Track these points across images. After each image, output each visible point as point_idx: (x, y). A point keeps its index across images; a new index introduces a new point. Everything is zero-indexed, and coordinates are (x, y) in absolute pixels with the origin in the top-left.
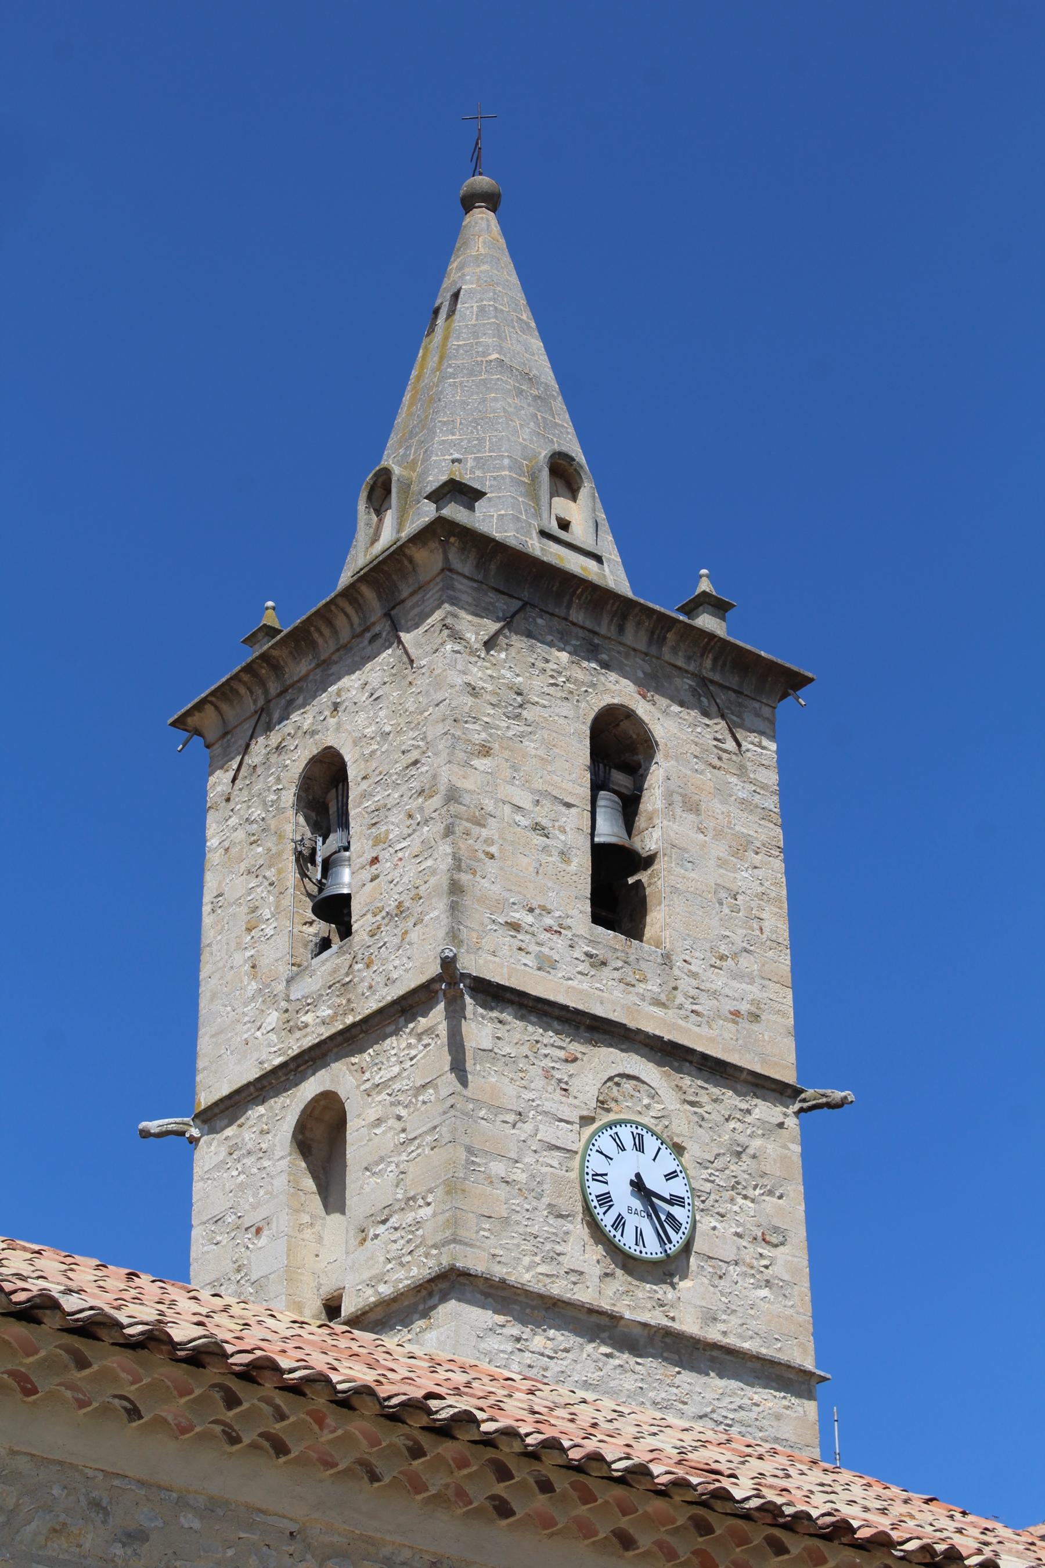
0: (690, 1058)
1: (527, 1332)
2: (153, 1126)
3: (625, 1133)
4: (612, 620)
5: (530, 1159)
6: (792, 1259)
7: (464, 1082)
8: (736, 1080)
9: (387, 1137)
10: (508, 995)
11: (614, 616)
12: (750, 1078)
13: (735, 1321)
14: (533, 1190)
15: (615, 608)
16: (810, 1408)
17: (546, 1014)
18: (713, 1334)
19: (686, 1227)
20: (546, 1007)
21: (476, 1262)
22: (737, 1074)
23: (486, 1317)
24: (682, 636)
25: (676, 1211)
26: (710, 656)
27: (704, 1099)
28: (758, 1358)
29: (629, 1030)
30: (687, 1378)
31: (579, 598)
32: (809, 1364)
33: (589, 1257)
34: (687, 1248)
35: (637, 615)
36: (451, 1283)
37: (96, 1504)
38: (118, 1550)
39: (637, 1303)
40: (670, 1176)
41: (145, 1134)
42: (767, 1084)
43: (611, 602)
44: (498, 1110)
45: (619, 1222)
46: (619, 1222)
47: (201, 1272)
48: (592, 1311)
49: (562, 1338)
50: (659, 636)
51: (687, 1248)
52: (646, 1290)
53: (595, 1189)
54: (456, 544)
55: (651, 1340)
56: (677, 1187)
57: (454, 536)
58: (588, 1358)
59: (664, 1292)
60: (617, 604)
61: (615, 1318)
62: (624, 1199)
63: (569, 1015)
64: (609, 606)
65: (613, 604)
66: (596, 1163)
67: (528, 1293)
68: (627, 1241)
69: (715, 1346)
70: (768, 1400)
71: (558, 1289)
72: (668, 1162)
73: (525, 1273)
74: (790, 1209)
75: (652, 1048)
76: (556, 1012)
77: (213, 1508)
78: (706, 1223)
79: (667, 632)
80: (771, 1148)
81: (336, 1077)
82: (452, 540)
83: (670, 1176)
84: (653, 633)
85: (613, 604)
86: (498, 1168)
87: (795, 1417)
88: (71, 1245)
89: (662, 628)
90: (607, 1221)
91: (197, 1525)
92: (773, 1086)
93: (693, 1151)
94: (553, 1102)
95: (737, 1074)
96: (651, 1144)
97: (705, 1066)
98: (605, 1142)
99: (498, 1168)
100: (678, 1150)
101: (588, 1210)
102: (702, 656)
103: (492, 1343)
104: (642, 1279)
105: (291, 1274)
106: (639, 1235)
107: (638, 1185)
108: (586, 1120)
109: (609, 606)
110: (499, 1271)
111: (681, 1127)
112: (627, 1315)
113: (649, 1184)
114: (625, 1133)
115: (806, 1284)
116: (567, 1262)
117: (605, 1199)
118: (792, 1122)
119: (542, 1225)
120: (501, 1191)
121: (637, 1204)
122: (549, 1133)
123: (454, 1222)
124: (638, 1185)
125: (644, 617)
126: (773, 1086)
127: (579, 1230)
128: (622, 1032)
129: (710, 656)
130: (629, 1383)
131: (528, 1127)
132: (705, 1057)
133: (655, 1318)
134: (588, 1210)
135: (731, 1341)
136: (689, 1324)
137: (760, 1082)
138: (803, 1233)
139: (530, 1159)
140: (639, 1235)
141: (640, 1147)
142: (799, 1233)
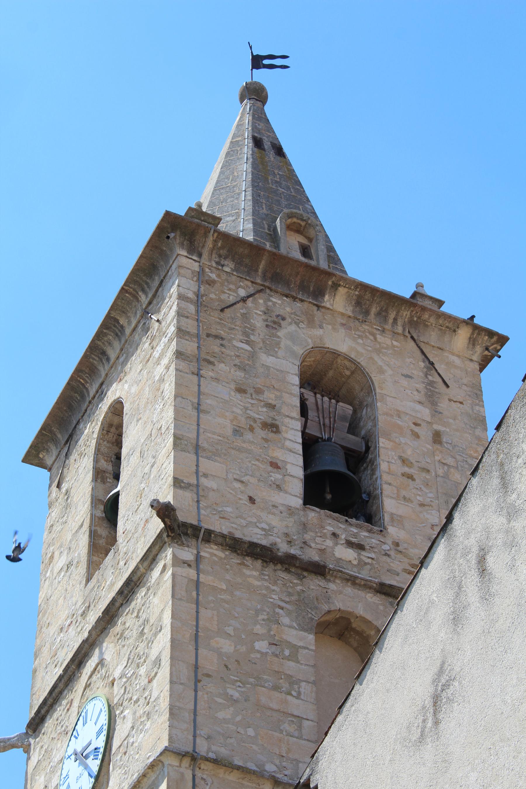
0: (117, 604)
4: (103, 364)
8: (143, 575)
10: (43, 712)
11: (102, 361)
12: (146, 564)
15: (97, 359)
17: (61, 693)
20: (57, 691)
22: (139, 574)
24: (123, 312)
26: (140, 293)
29: (87, 639)
31: (87, 382)
35: (103, 343)
42: (154, 551)
43: (91, 360)
50: (120, 331)
54: (44, 454)
57: (38, 454)
60: (93, 356)
63: (66, 678)
64: (95, 362)
65: (94, 359)
75: (105, 629)
76: (61, 685)
79: (118, 323)
82: (41, 456)
84: (117, 335)
85: (94, 359)
89: (115, 326)
92: (157, 547)
95: (139, 574)
97: (128, 595)
102: (138, 301)
109: (95, 362)
125: (106, 339)
126: (157, 547)
128: (86, 646)
129: (140, 293)
132: (120, 592)
137: (151, 557)
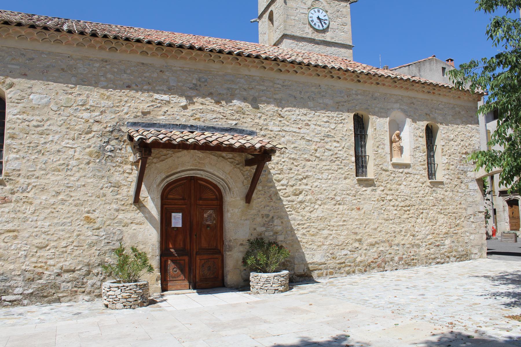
1: (298, 43)
2: (252, 20)
3: (316, 10)
5: (298, 16)
6: (348, 28)
7: (286, 4)
9: (277, 15)
13: (337, 38)
14: (299, 20)
16: (351, 51)
18: (333, 41)
19: (328, 24)
21: (288, 33)
23: (291, 41)
25: (325, 21)
27: (331, 3)
28: (341, 44)
30: (328, 48)
32: (351, 44)
33: (309, 30)
34: (328, 27)
36: (285, 36)
37: (23, 54)
38: (28, 61)
39: (319, 37)
40: (324, 16)
41: (251, 22)
44: (292, 8)
45: (315, 24)
46: (315, 24)
47: (260, 41)
48: (310, 39)
49: (305, 43)
51: (328, 27)
52: (320, 35)
53: (310, 19)
55: (321, 42)
56: (326, 18)
58: (310, 46)
59: (323, 35)
61: (314, 40)
62: (316, 20)
66: (310, 15)
67: (298, 37)
68: (317, 27)
69: (333, 42)
70: (343, 50)
71: (304, 36)
72: (324, 13)
73: (298, 34)
74: (348, 20)
77: (50, 53)
78: (331, 23)
80: (344, 10)
81: (272, 8)
83: (324, 16)
86: (293, 17)
87: (348, 53)
88: (173, 30)
90: (313, 24)
91: (46, 56)
93: (329, 11)
94: (303, 6)
96: (321, 11)
98: (312, 11)
99: (293, 17)
100: (327, 12)
101: (309, 23)
103: (292, 45)
104: (320, 33)
105: (269, 40)
106: (319, 26)
107: (318, 18)
108: (309, 8)
110: (293, 34)
111: (327, 7)
112: (317, 39)
113: (320, 17)
114: (316, 10)
115: (351, 31)
116: (306, 31)
117: (312, 21)
118: (348, 5)
119: (301, 26)
120: (293, 21)
121: (319, 21)
122: (302, 11)
123: (285, 27)
124: (318, 18)
127: (308, 26)
130: (317, 49)
131: (298, 10)
133: (323, 39)
134: (309, 23)
135: (336, 41)
136: (328, 39)
138: (350, 23)
139: (298, 16)
140: (319, 26)
141: (319, 11)
142: (349, 23)
